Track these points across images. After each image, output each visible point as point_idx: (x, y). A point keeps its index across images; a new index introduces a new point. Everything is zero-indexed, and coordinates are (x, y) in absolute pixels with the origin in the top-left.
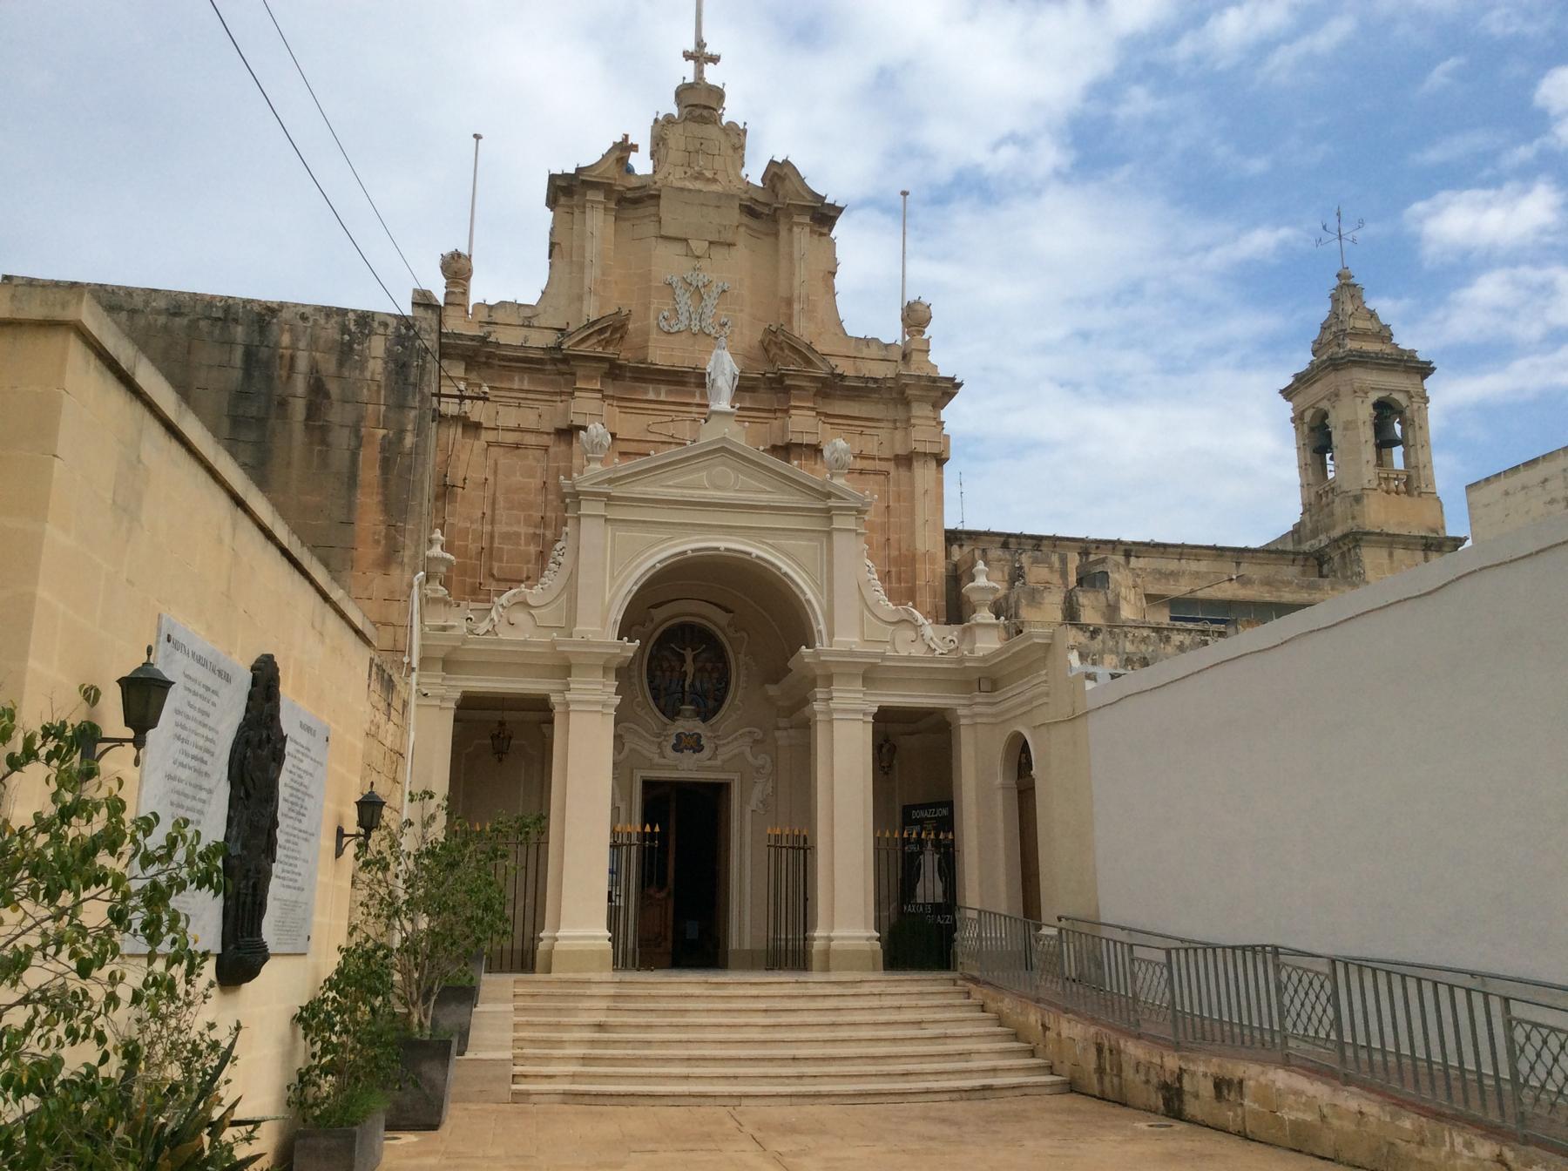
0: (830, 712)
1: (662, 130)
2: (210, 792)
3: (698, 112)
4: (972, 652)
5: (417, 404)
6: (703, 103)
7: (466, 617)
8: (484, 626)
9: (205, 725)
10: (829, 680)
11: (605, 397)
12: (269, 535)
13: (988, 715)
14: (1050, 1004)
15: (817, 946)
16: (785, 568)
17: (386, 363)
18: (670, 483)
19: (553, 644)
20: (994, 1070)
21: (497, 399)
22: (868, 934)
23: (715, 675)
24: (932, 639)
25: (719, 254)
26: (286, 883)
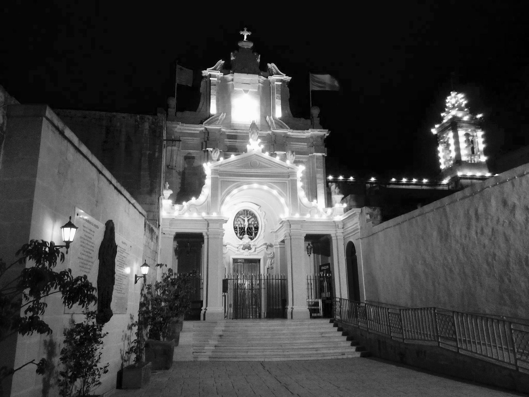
2: (93, 263)
9: (90, 242)
12: (111, 183)
26: (118, 291)
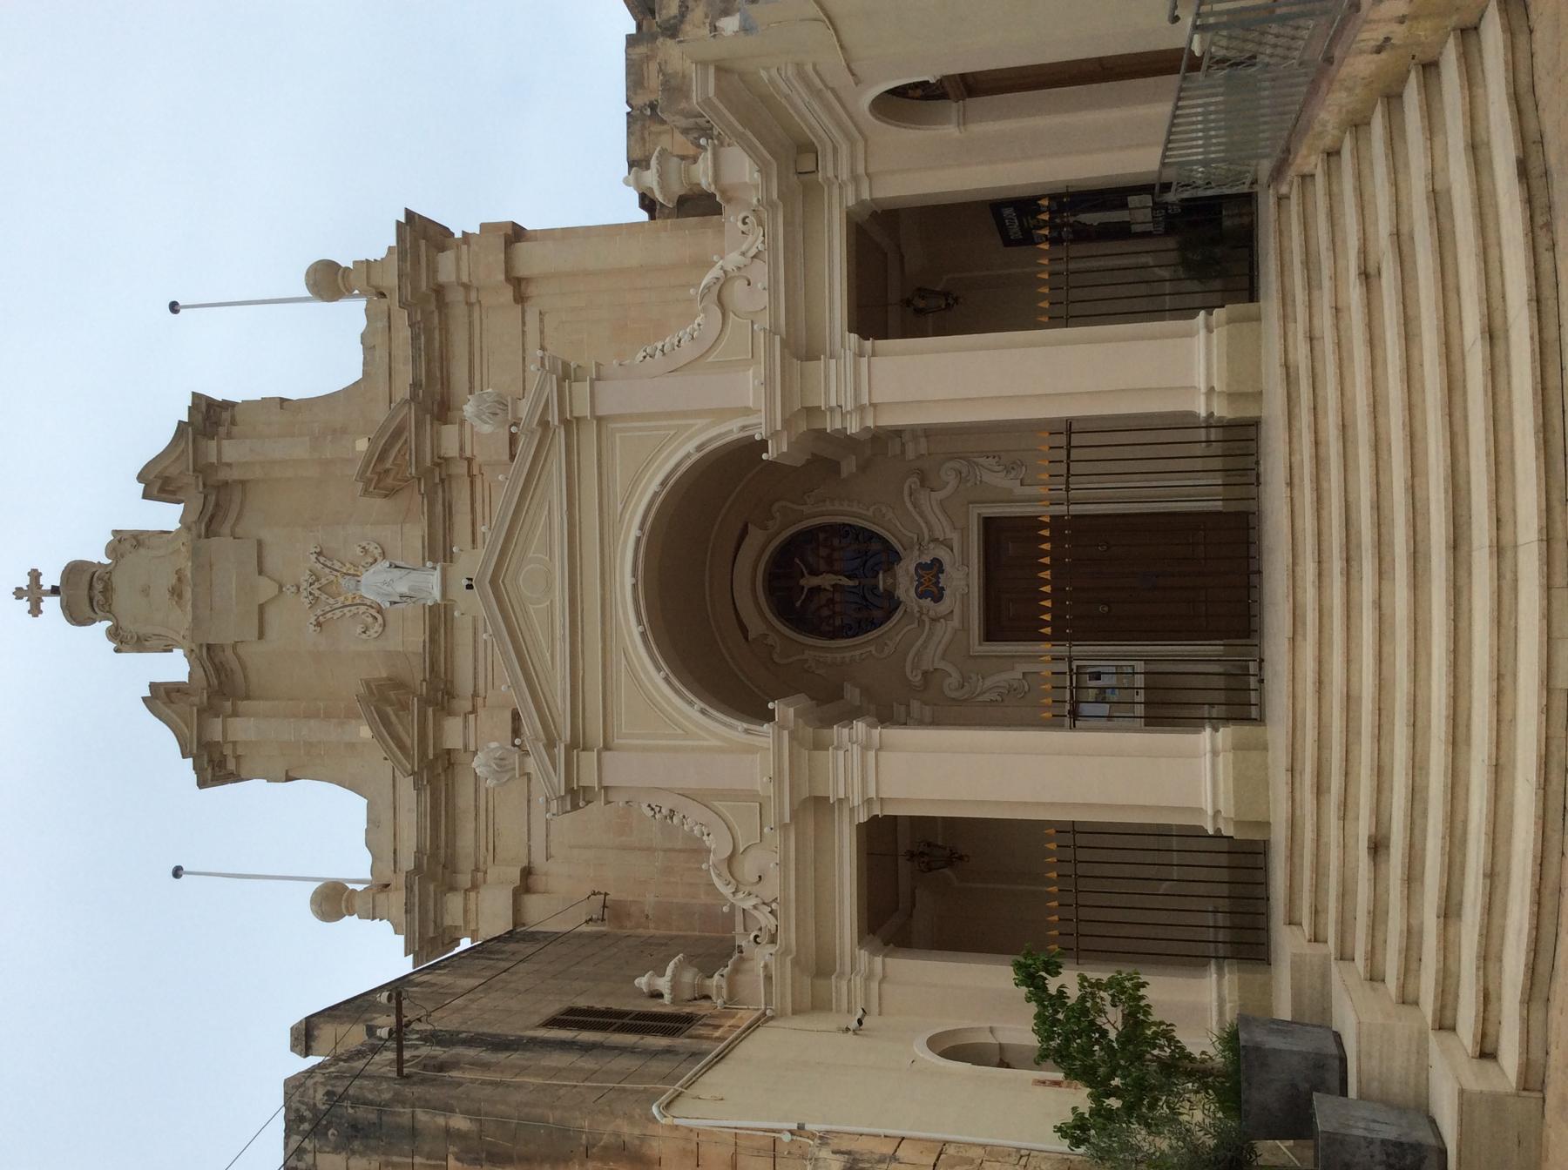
0: (861, 409)
3: (98, 597)
4: (756, 187)
5: (408, 1110)
6: (86, 592)
7: (752, 943)
8: (764, 919)
10: (811, 412)
11: (474, 711)
13: (853, 157)
14: (1333, 41)
15: (1222, 410)
16: (654, 486)
17: (353, 1152)
18: (548, 655)
19: (784, 827)
20: (1476, 149)
21: (491, 847)
22: (1202, 333)
23: (836, 542)
24: (743, 254)
25: (273, 561)
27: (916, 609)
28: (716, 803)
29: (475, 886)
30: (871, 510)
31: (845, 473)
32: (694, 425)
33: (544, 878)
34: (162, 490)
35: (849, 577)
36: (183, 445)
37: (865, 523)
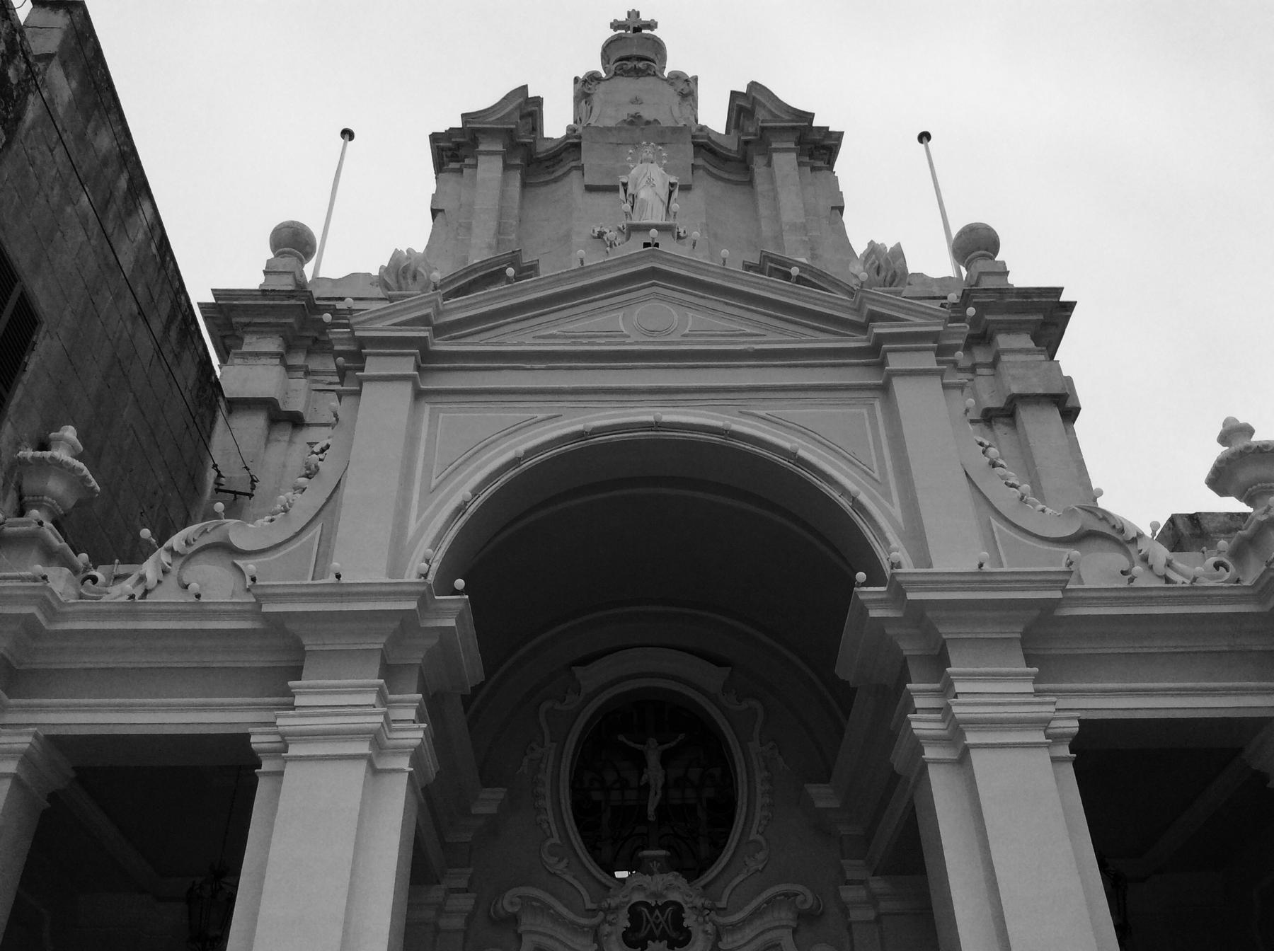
0: (955, 732)
1: (586, 88)
3: (630, 65)
10: (938, 661)
18: (555, 331)
27: (613, 902)
28: (319, 528)
29: (289, 369)
30: (759, 838)
31: (813, 789)
32: (892, 504)
33: (286, 438)
34: (741, 110)
35: (659, 809)
36: (787, 118)
37: (734, 844)
